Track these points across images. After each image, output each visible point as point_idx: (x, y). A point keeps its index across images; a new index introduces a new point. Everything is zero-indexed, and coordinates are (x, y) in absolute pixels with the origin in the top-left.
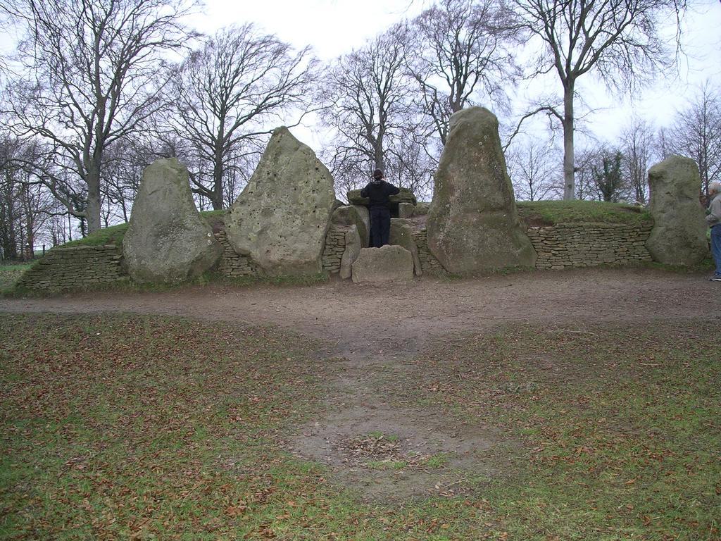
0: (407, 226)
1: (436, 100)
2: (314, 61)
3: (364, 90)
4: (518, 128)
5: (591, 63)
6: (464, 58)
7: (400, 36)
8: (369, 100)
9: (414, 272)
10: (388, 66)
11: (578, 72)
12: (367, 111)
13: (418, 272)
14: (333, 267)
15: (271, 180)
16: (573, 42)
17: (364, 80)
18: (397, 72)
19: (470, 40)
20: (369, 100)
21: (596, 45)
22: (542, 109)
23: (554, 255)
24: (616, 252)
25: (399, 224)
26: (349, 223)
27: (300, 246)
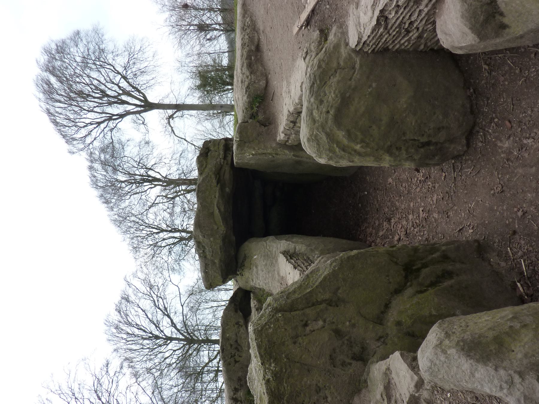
1: (166, 197)
2: (135, 275)
3: (157, 242)
4: (182, 138)
5: (139, 91)
6: (138, 177)
7: (121, 220)
8: (164, 239)
10: (142, 227)
11: (145, 100)
12: (171, 241)
16: (124, 102)
17: (151, 243)
18: (147, 221)
19: (125, 174)
20: (164, 239)
21: (129, 88)
22: (169, 123)
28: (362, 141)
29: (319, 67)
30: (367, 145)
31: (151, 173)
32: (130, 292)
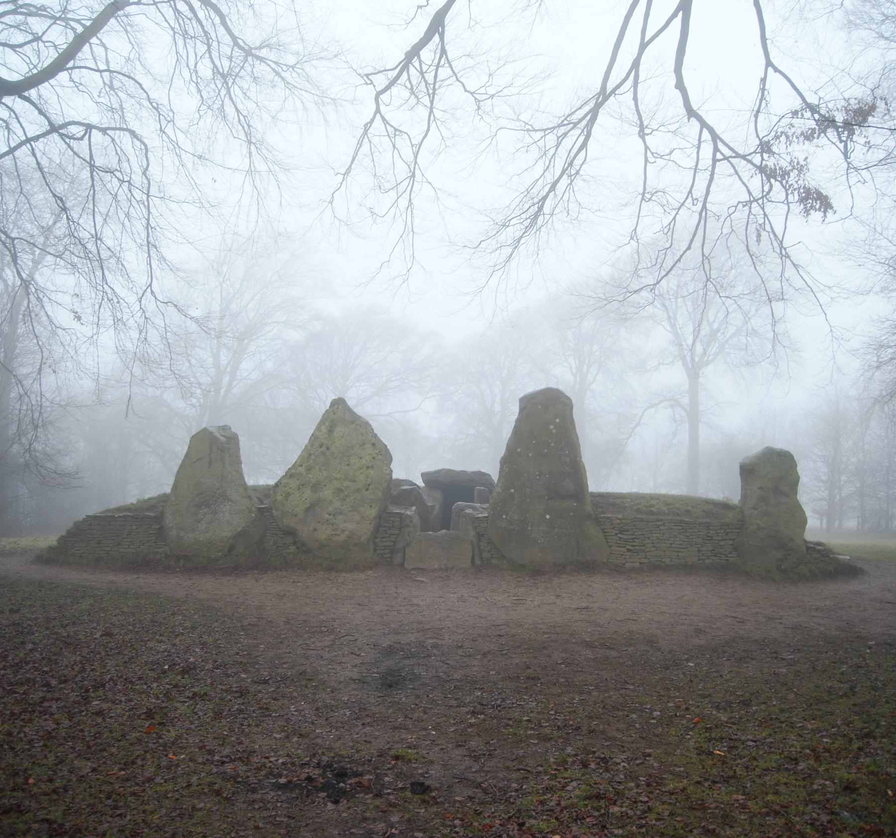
13: (478, 562)
14: (386, 551)
15: (324, 454)
23: (629, 550)
24: (699, 551)
27: (350, 526)
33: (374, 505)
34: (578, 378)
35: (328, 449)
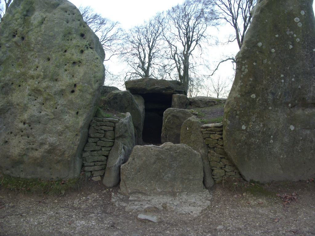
0: (193, 118)
3: (142, 45)
4: (218, 67)
8: (144, 50)
9: (204, 182)
12: (142, 55)
13: (210, 182)
17: (142, 41)
19: (194, 25)
20: (144, 50)
22: (229, 59)
25: (180, 114)
26: (123, 109)
28: (168, 121)
29: (187, 112)
30: (166, 123)
31: (194, 43)
32: (108, 25)
33: (80, 113)
34: (186, 47)
35: (23, 38)
